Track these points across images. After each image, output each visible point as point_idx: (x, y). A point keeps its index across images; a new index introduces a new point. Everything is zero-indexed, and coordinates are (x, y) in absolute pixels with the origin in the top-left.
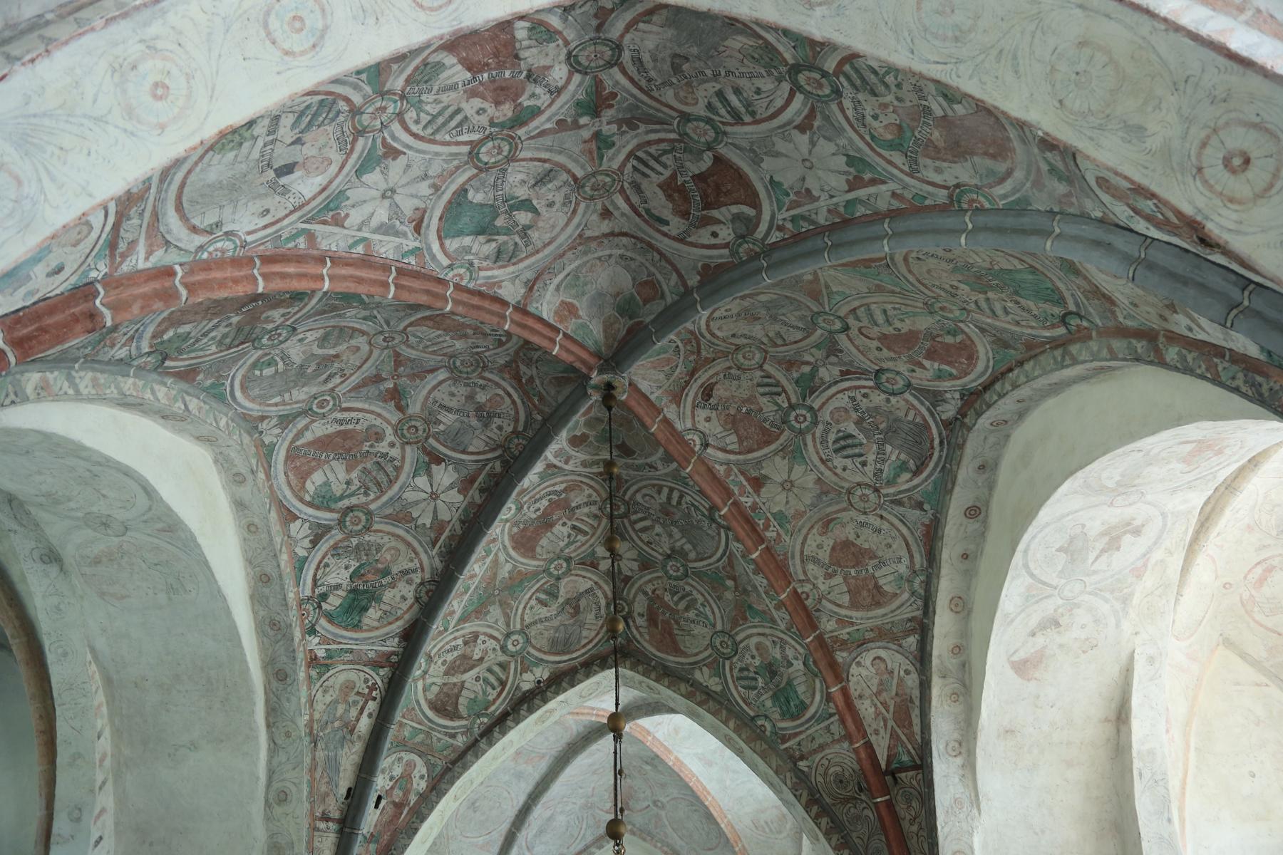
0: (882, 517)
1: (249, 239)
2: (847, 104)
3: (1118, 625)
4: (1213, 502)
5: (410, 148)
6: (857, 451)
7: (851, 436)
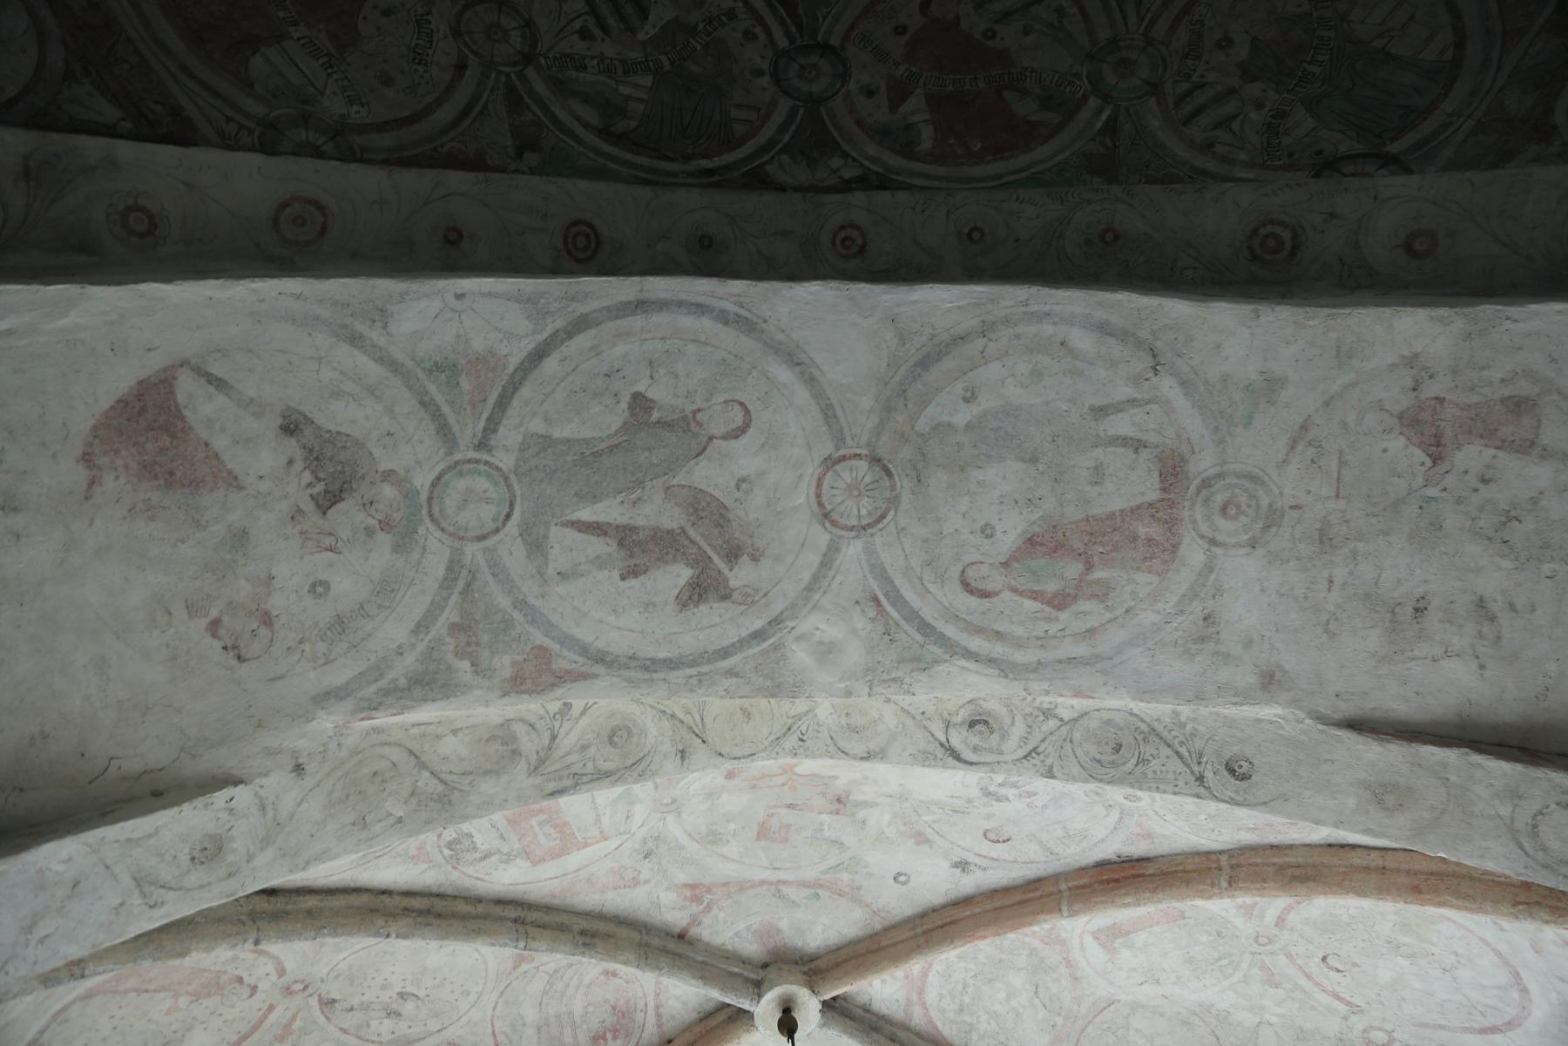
0: (461, 67)
3: (325, 698)
4: (481, 908)
6: (612, 22)
7: (644, 13)
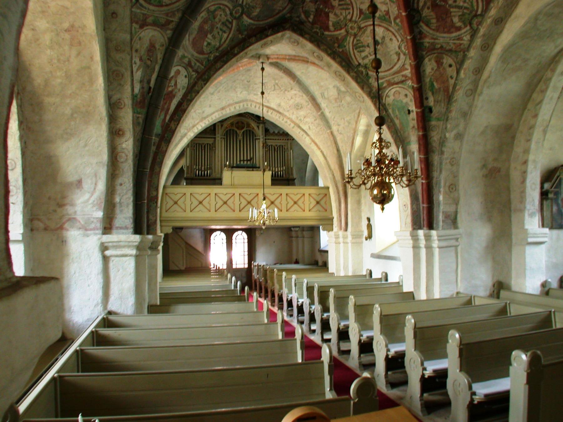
1: (400, 40)
2: (228, 12)
5: (357, 7)
